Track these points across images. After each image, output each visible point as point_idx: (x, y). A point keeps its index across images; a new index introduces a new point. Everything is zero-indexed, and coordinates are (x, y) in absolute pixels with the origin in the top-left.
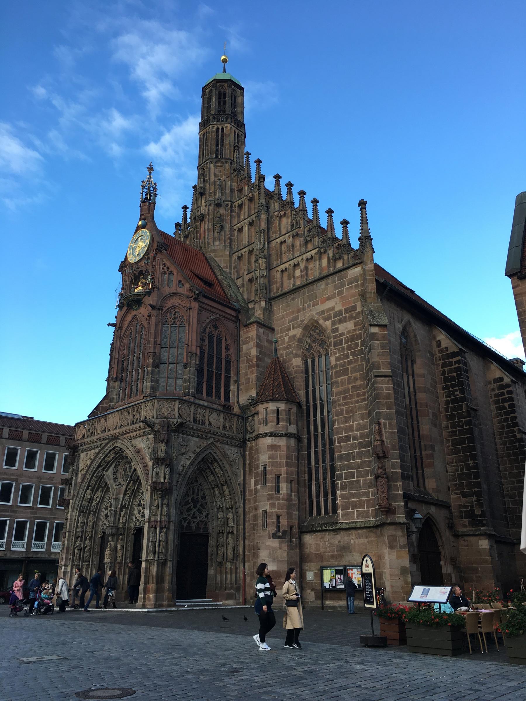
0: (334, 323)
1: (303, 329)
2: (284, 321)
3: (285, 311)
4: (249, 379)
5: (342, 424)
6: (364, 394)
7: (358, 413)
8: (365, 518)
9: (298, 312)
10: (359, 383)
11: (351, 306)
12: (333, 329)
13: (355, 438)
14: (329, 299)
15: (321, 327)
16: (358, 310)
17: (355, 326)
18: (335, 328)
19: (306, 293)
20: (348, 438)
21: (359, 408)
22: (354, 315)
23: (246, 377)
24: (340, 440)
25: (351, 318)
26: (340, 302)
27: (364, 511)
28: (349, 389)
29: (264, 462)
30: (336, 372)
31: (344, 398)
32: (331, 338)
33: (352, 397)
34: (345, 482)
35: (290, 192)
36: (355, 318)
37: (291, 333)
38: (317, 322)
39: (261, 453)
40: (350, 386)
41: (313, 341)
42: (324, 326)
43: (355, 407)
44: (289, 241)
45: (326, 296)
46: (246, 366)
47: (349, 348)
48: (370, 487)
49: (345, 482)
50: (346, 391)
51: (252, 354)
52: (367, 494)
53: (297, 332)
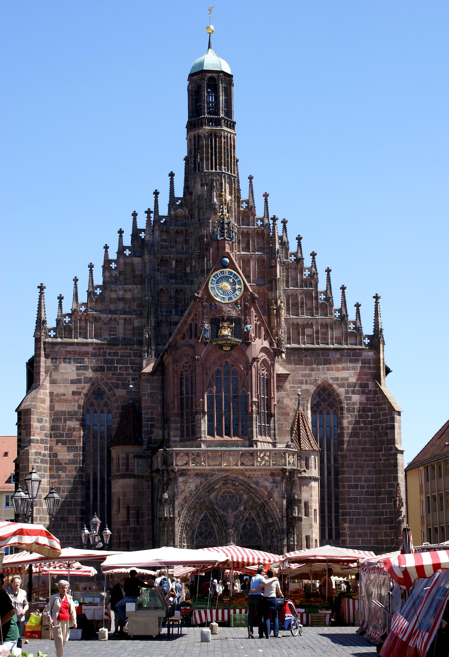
0: (347, 392)
4: (282, 424)
5: (352, 475)
6: (372, 456)
7: (366, 469)
8: (368, 544)
10: (368, 446)
11: (364, 383)
12: (347, 397)
13: (362, 487)
15: (334, 390)
16: (370, 388)
17: (367, 400)
20: (356, 486)
21: (367, 466)
22: (367, 391)
24: (350, 487)
25: (363, 393)
26: (354, 376)
27: (367, 540)
28: (359, 449)
29: (306, 499)
30: (348, 433)
31: (355, 455)
32: (344, 404)
33: (361, 455)
34: (353, 518)
35: (299, 245)
36: (367, 394)
38: (331, 385)
39: (303, 491)
40: (360, 447)
43: (364, 464)
47: (360, 416)
48: (373, 524)
49: (353, 518)
50: (356, 450)
51: (284, 403)
52: (370, 528)
53: (312, 388)
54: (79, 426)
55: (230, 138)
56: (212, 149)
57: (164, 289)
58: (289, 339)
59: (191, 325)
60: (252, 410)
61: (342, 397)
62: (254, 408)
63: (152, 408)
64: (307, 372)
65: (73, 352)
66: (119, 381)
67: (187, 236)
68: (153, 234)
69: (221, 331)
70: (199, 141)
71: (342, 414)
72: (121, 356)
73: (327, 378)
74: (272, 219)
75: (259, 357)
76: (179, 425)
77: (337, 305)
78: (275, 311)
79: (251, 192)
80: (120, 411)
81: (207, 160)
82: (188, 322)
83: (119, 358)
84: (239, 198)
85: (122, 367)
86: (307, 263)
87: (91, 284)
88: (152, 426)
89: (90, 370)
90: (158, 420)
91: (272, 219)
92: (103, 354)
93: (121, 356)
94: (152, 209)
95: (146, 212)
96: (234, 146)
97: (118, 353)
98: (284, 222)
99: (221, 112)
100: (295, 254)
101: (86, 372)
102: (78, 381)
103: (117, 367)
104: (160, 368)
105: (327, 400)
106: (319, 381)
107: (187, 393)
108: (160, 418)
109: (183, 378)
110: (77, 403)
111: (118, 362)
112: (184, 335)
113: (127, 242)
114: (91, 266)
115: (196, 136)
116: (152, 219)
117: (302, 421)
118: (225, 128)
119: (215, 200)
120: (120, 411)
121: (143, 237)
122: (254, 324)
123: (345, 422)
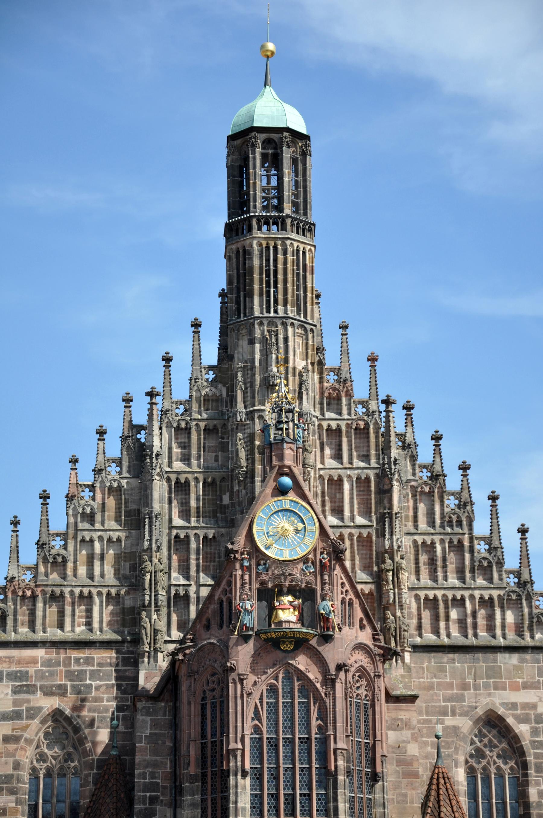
1: (474, 723)
2: (432, 695)
3: (435, 677)
4: (405, 795)
9: (465, 690)
12: (534, 742)
14: (526, 686)
18: (537, 741)
19: (482, 661)
23: (398, 791)
32: (530, 756)
37: (449, 721)
38: (501, 719)
41: (485, 746)
42: (517, 731)
44: (439, 548)
45: (521, 681)
46: (397, 772)
53: (465, 725)
54: (13, 805)
55: (304, 253)
56: (268, 276)
57: (182, 536)
58: (419, 627)
59: (221, 603)
60: (336, 767)
61: (526, 743)
62: (341, 763)
63: (155, 765)
64: (455, 691)
65: (7, 660)
66: (94, 711)
67: (225, 436)
68: (161, 434)
69: (277, 614)
70: (245, 259)
71: (526, 775)
72: (99, 664)
73: (494, 704)
74: (383, 402)
75: (349, 662)
76: (198, 797)
77: (512, 562)
78: (390, 574)
79: (345, 352)
80: (95, 771)
81: (261, 295)
82: (216, 597)
83: (95, 668)
84: (321, 363)
85: (100, 686)
86: (453, 482)
87: (44, 530)
88: (153, 800)
89: (39, 692)
90: (164, 787)
91: (383, 402)
92: (64, 661)
93: (99, 664)
94: (159, 388)
95: (148, 394)
96: (312, 267)
97: (93, 658)
98: (408, 408)
99: (286, 205)
100: (429, 467)
101: (31, 697)
102: (16, 716)
103: (91, 685)
104: (170, 686)
105: (496, 746)
106: (478, 710)
107: (213, 735)
108: (167, 784)
109: (206, 704)
110: (11, 760)
111: (94, 675)
112: (209, 621)
113: (114, 447)
114: (45, 497)
115: (241, 251)
116: (159, 407)
117: (444, 789)
118: (293, 236)
119: (275, 369)
120: (95, 771)
121: (143, 440)
122: (340, 599)
123: (533, 793)
